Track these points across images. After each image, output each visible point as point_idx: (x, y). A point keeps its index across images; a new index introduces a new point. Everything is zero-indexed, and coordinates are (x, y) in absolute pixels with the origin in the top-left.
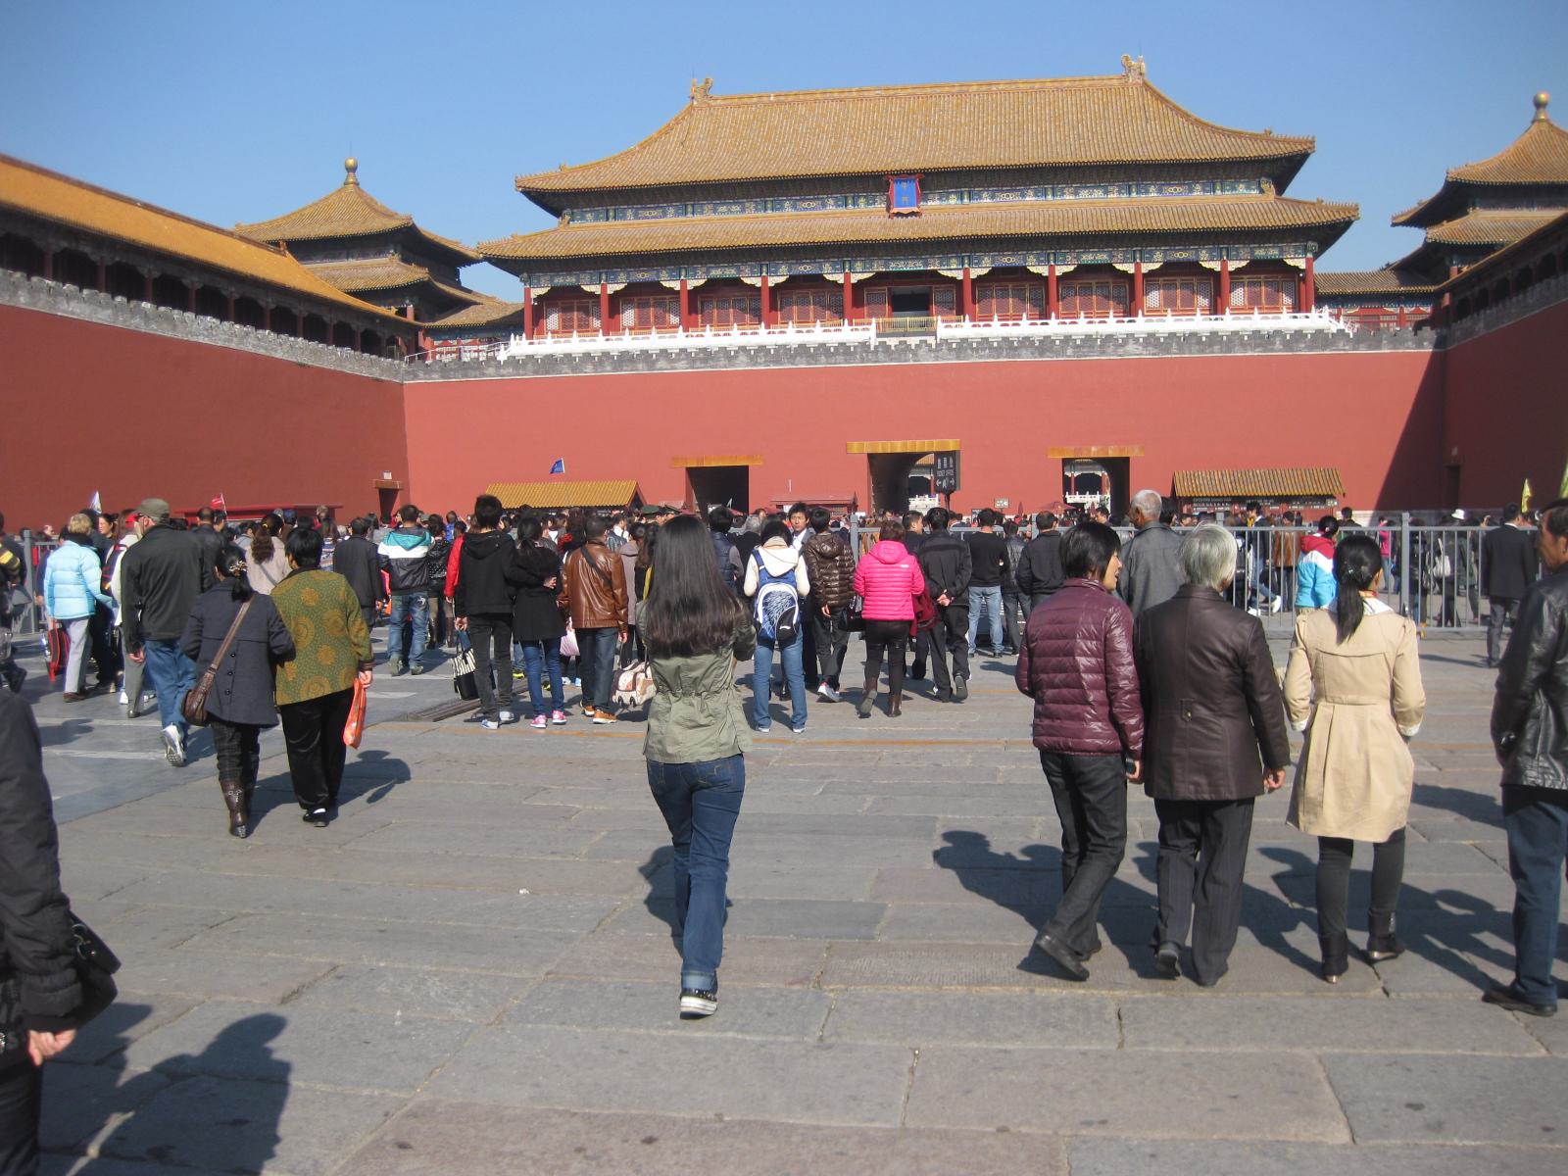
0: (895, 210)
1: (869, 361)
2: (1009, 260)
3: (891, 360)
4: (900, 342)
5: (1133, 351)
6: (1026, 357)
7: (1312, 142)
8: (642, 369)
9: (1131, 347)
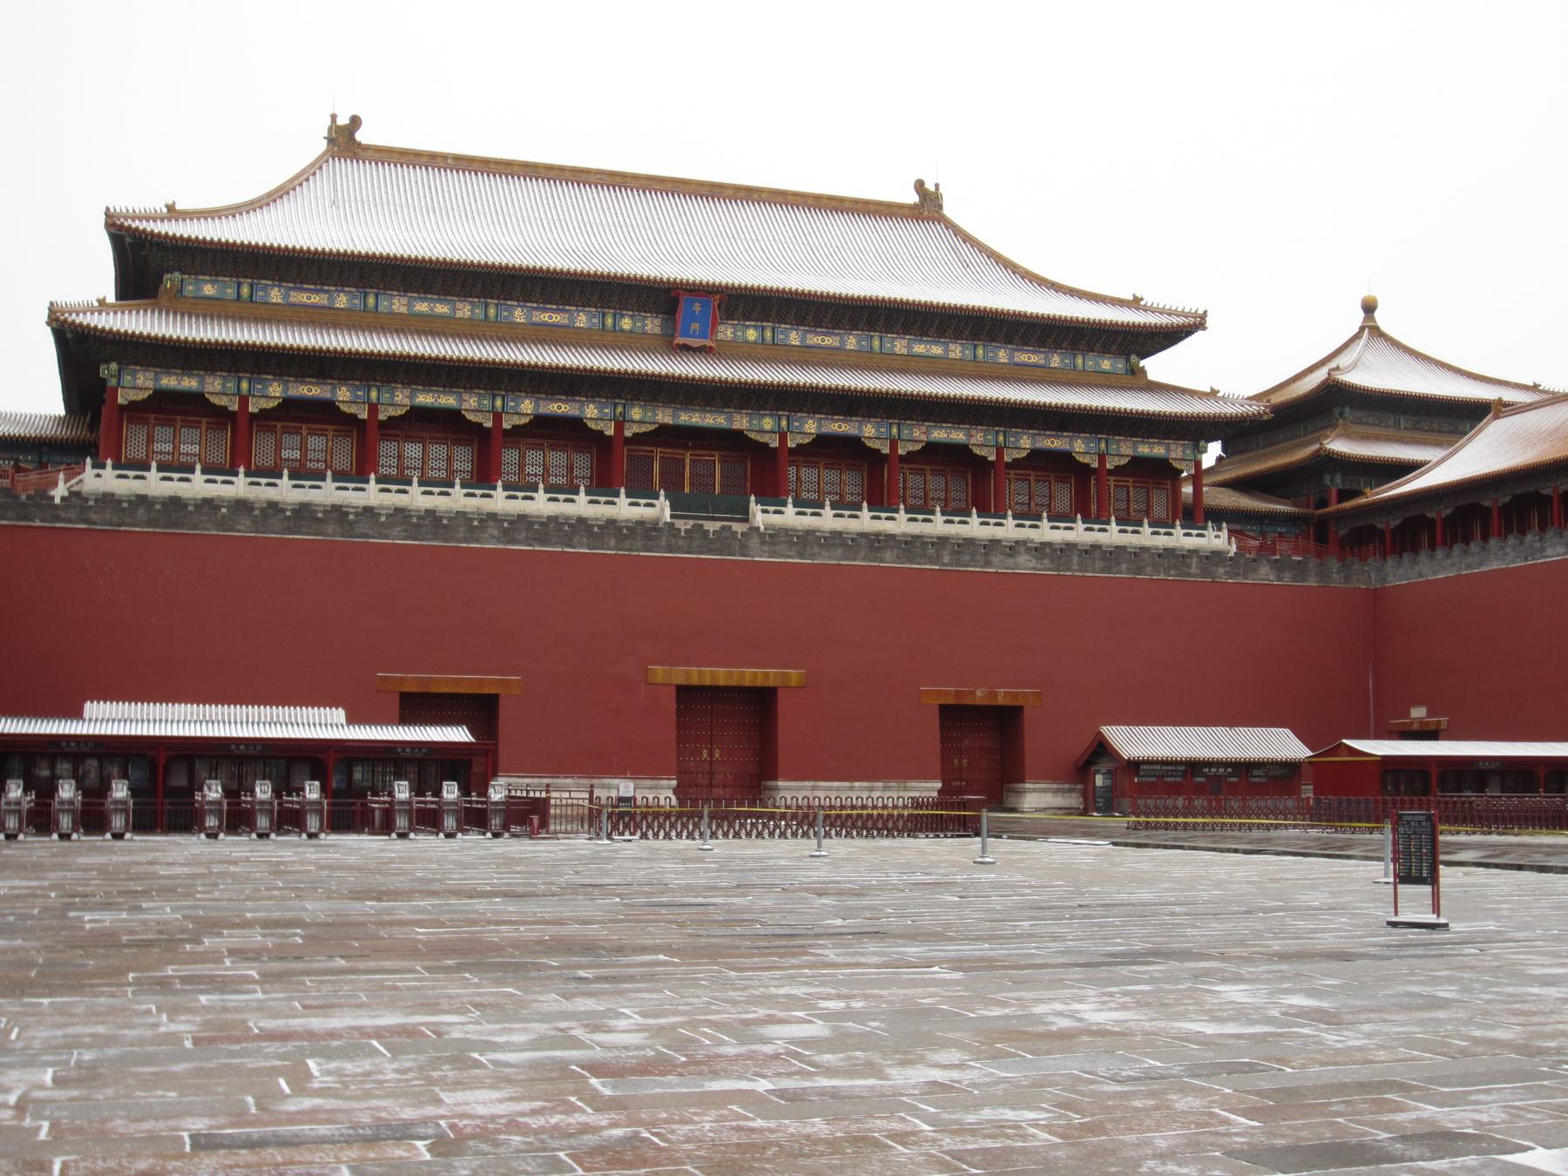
0: (680, 340)
1: (679, 550)
2: (839, 427)
3: (710, 552)
4: (723, 528)
5: (1025, 564)
6: (889, 561)
7: (1204, 316)
8: (332, 534)
9: (1023, 558)
